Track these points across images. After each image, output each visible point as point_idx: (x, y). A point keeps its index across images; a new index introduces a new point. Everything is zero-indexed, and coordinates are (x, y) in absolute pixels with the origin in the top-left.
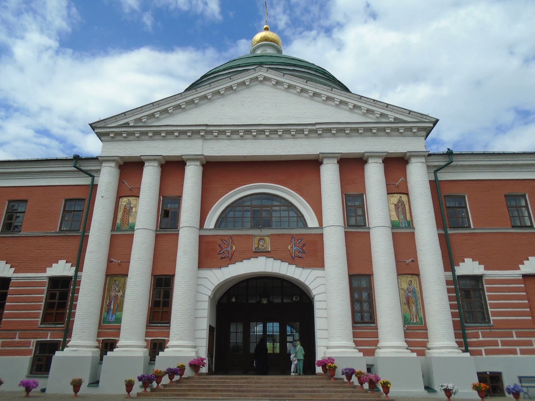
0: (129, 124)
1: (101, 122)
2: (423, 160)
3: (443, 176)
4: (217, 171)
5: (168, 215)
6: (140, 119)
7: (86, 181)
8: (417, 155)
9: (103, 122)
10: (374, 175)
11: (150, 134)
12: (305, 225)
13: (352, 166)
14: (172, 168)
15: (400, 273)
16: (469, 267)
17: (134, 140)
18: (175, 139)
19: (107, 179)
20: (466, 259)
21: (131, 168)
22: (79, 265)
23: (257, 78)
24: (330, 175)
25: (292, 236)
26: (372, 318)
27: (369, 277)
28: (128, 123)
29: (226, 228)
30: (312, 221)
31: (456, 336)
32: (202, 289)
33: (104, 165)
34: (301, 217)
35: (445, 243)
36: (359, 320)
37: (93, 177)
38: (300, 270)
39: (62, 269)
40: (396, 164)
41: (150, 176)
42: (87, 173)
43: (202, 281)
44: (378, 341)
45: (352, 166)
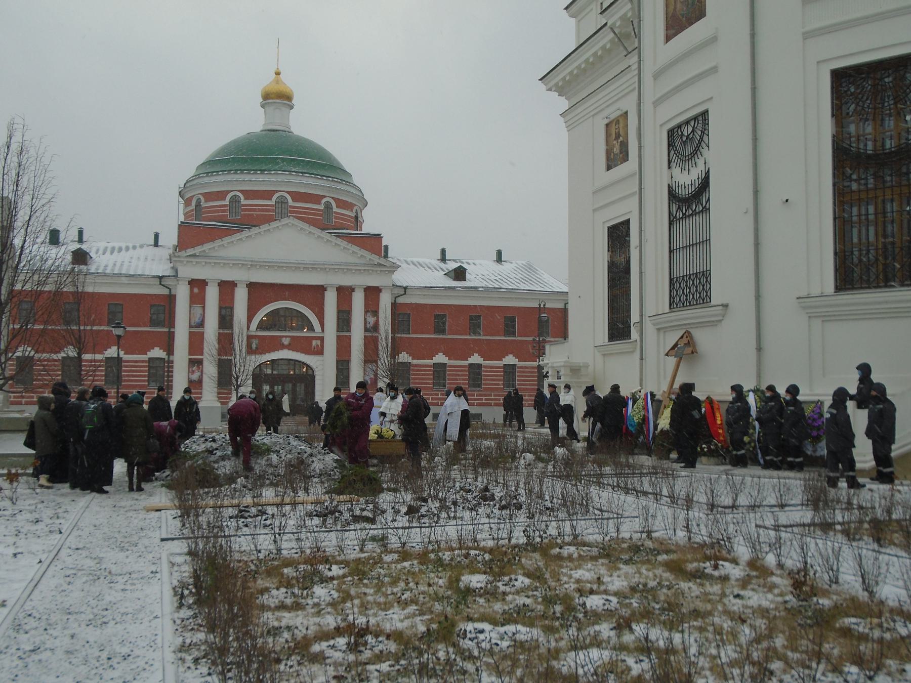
3: (400, 300)
4: (260, 293)
5: (226, 320)
6: (204, 251)
7: (165, 292)
12: (311, 329)
13: (345, 293)
14: (227, 288)
15: (366, 362)
19: (182, 294)
21: (198, 286)
22: (170, 350)
39: (157, 353)
40: (372, 293)
45: (345, 293)
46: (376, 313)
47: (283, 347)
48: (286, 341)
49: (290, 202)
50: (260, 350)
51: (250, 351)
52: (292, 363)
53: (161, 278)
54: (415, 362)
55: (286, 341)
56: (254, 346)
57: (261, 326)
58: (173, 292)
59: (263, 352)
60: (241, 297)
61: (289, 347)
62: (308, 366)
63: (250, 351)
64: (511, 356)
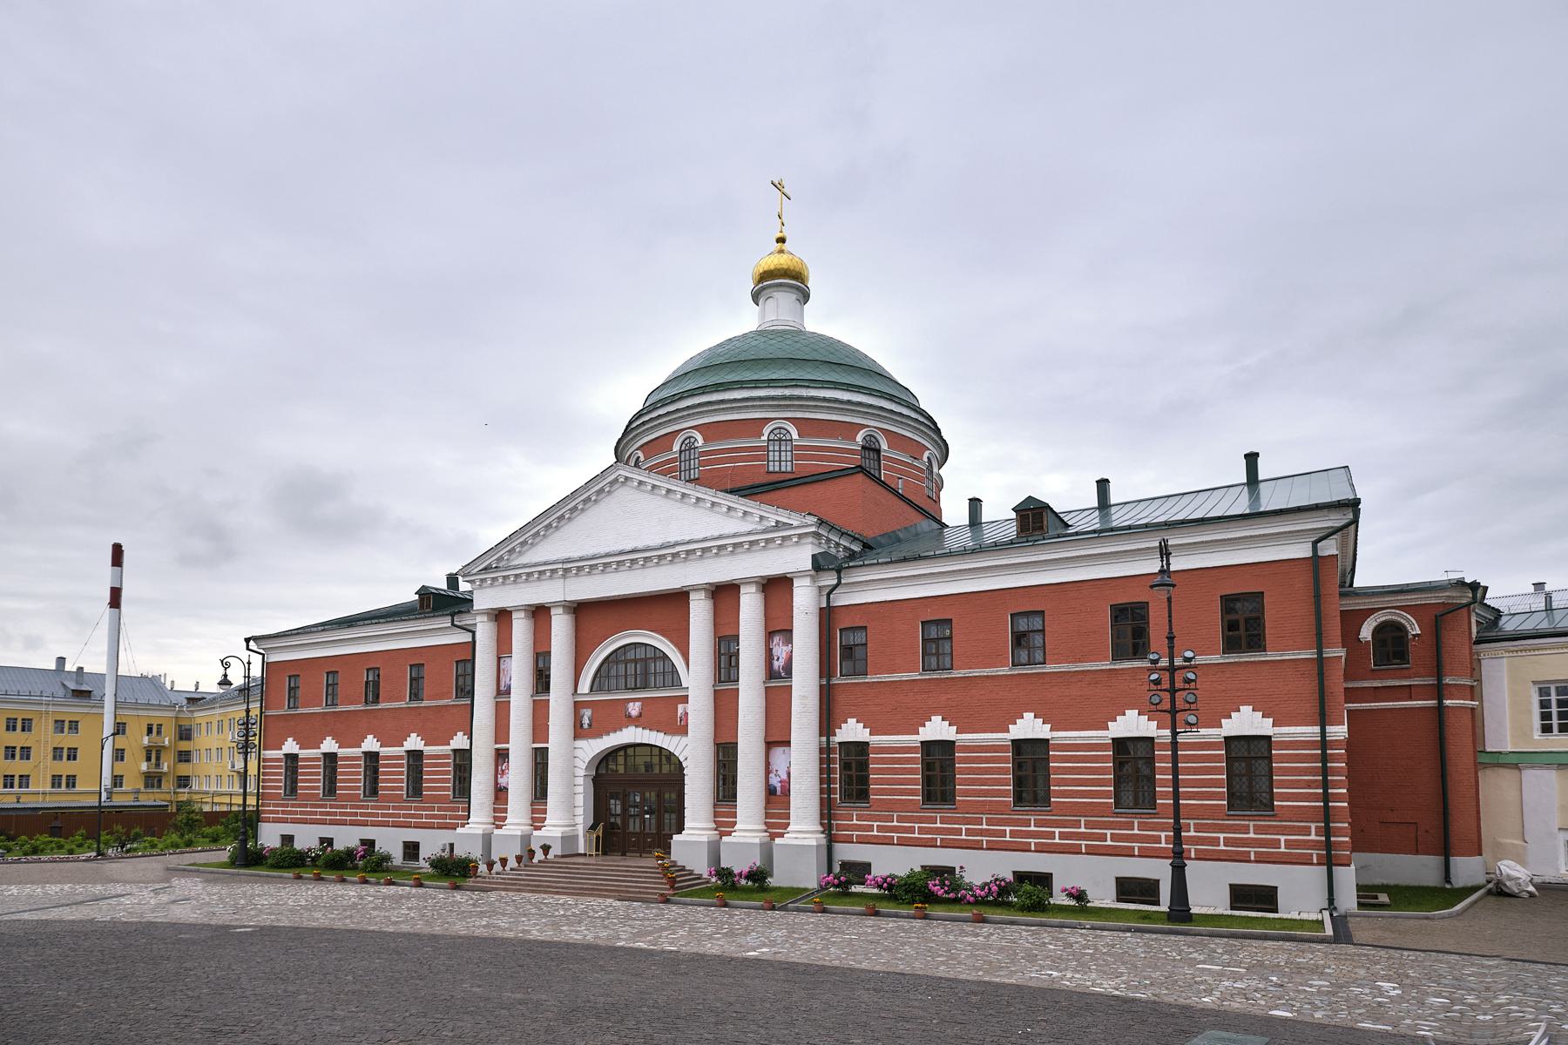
2: (807, 581)
3: (842, 599)
8: (801, 574)
10: (750, 605)
16: (852, 731)
19: (485, 632)
20: (852, 721)
24: (700, 612)
27: (734, 746)
29: (600, 690)
31: (822, 816)
32: (578, 763)
35: (827, 696)
37: (474, 633)
38: (668, 738)
41: (521, 628)
43: (578, 753)
44: (735, 823)
46: (787, 633)
47: (630, 721)
48: (634, 709)
50: (595, 731)
51: (579, 732)
52: (656, 752)
54: (877, 740)
55: (634, 709)
56: (586, 721)
57: (598, 683)
59: (599, 735)
60: (561, 626)
61: (638, 721)
62: (670, 755)
63: (579, 732)
64: (1132, 714)
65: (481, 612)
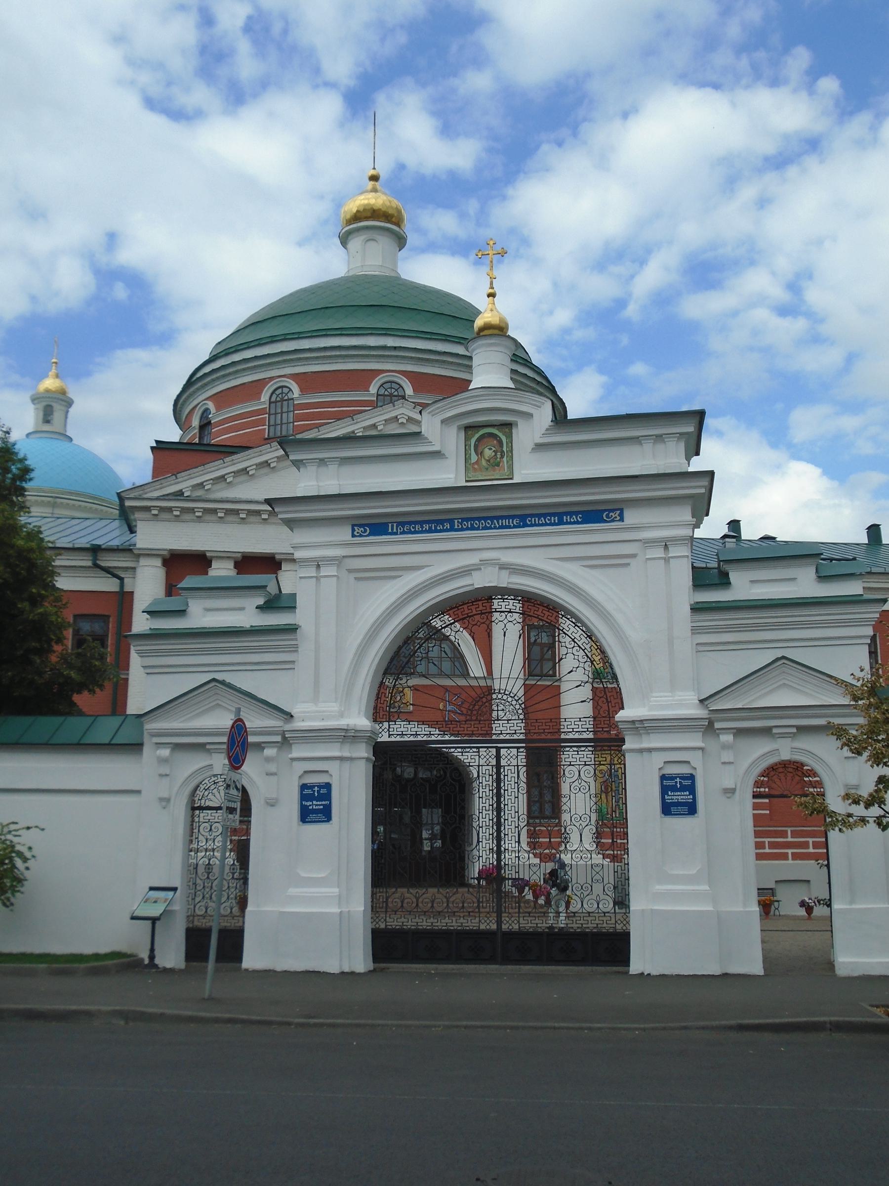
0: (183, 494)
1: (137, 490)
6: (201, 485)
7: (108, 585)
9: (140, 489)
11: (220, 515)
17: (193, 521)
18: (261, 523)
23: (396, 418)
25: (446, 689)
26: (556, 811)
28: (180, 493)
30: (476, 668)
33: (143, 561)
34: (459, 658)
36: (537, 814)
42: (109, 572)
49: (409, 391)
53: (95, 550)
58: (127, 589)
65: (150, 554)
